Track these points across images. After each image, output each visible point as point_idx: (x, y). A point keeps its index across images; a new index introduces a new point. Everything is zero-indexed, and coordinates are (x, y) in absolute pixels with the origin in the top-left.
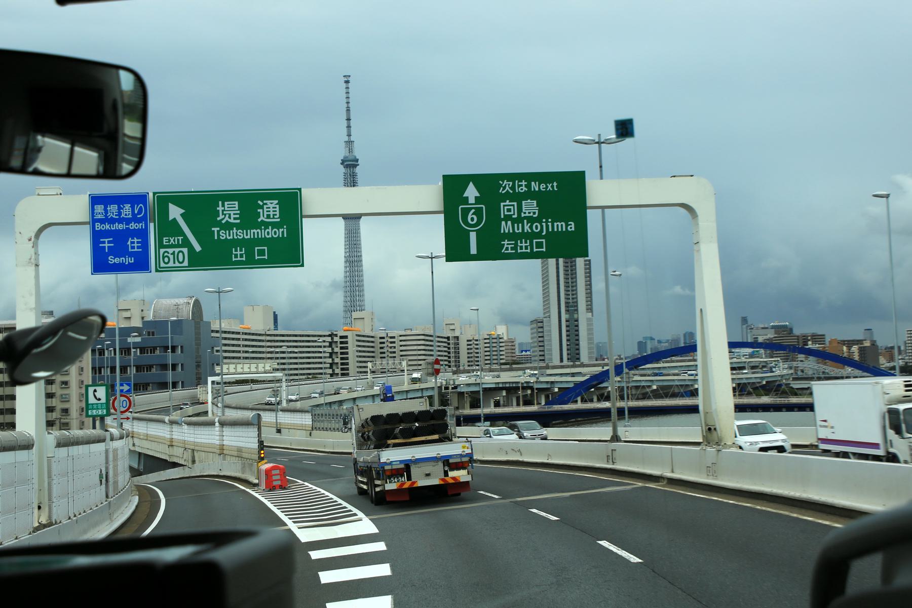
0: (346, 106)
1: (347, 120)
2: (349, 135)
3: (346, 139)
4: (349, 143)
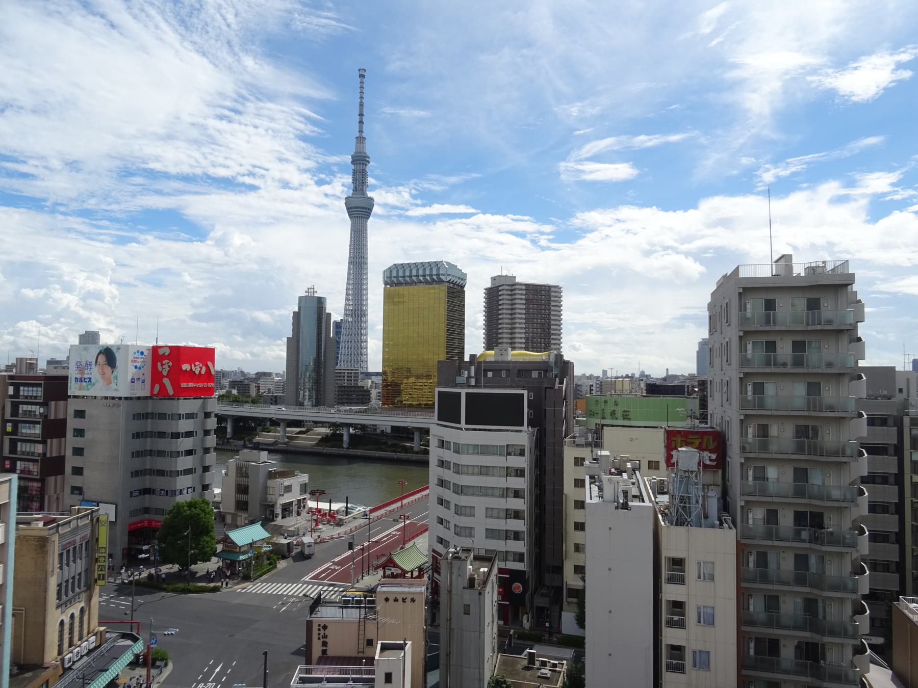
0: (359, 101)
1: (359, 115)
2: (361, 131)
3: (358, 135)
4: (361, 139)
